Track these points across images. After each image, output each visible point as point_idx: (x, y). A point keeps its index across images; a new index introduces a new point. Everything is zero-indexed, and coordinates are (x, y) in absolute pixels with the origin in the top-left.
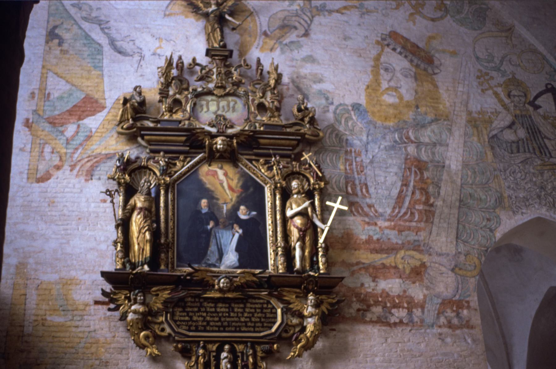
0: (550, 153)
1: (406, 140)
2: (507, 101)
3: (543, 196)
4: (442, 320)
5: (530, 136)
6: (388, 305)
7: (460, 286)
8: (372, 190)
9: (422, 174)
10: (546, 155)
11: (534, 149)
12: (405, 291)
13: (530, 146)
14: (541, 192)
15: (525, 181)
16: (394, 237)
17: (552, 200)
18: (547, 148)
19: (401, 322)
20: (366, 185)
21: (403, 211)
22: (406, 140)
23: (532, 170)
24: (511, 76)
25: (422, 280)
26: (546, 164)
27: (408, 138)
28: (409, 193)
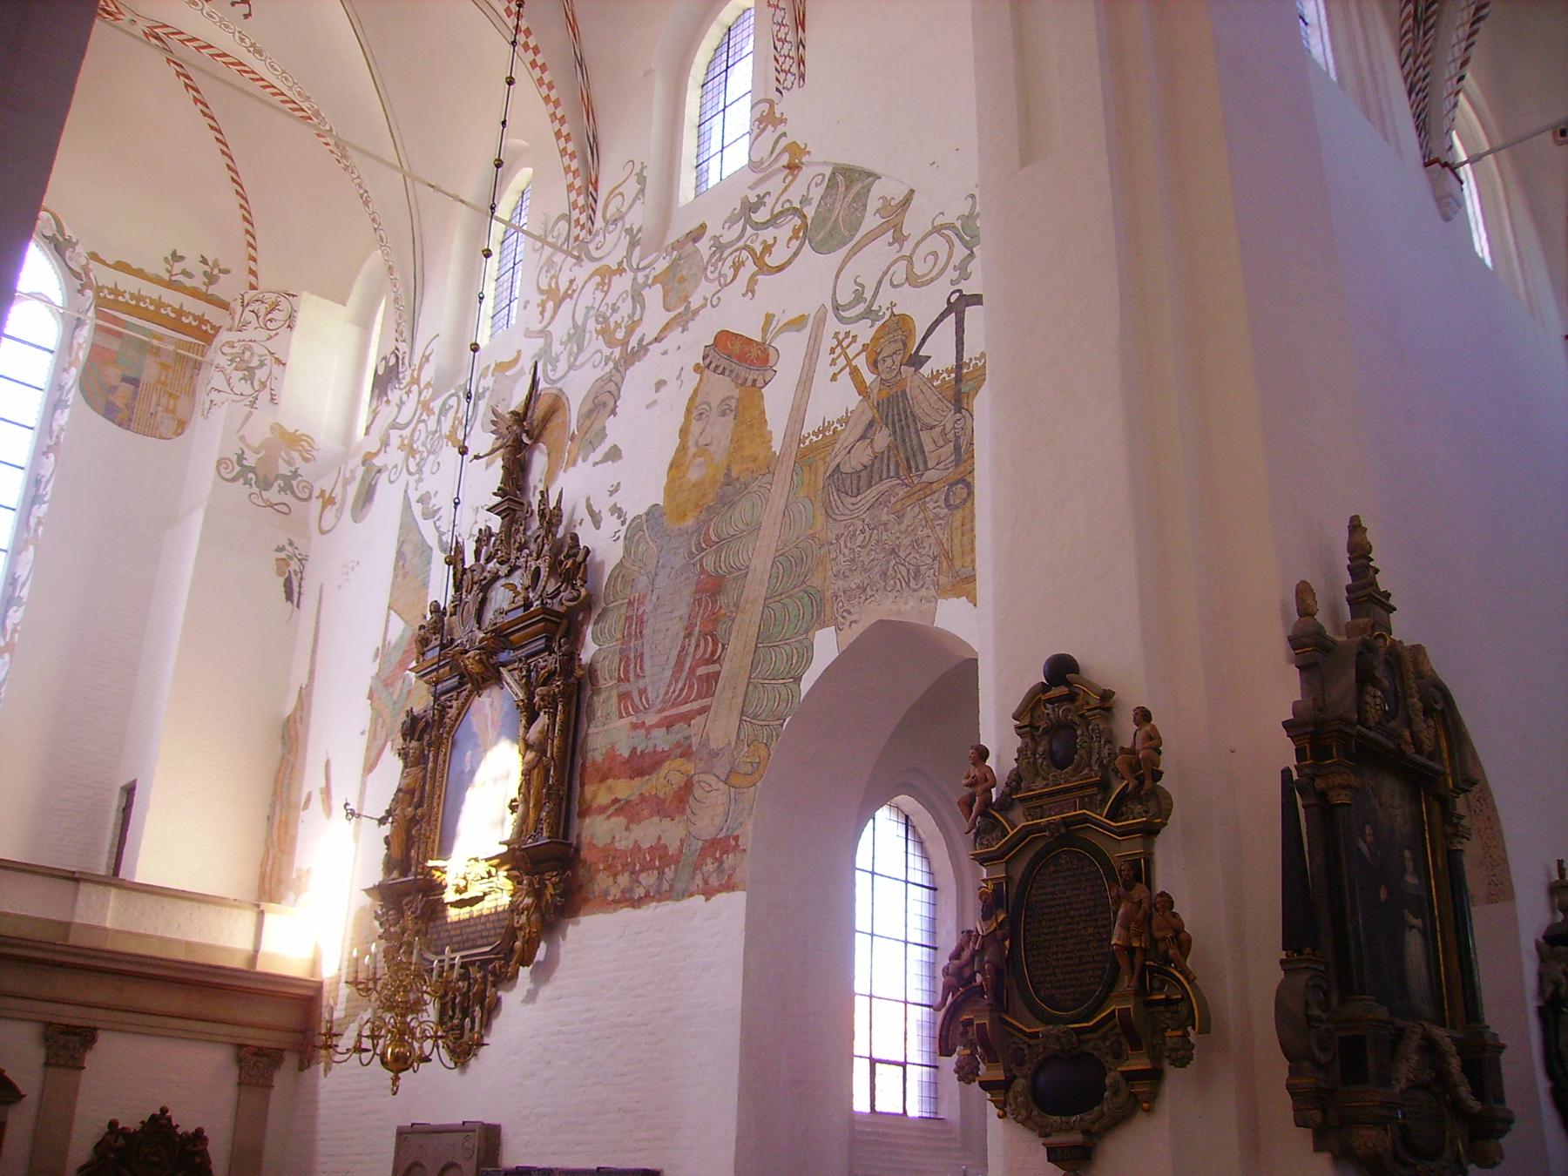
0: (925, 463)
1: (704, 545)
2: (869, 377)
3: (890, 572)
4: (699, 880)
5: (896, 440)
6: (637, 868)
7: (731, 809)
8: (647, 665)
9: (715, 602)
10: (917, 469)
11: (897, 464)
12: (660, 838)
13: (892, 460)
14: (889, 562)
15: (869, 547)
16: (662, 740)
17: (905, 574)
18: (923, 452)
19: (647, 895)
20: (642, 654)
21: (680, 685)
22: (704, 545)
23: (884, 518)
24: (888, 314)
25: (683, 811)
26: (915, 489)
27: (707, 540)
28: (692, 649)
